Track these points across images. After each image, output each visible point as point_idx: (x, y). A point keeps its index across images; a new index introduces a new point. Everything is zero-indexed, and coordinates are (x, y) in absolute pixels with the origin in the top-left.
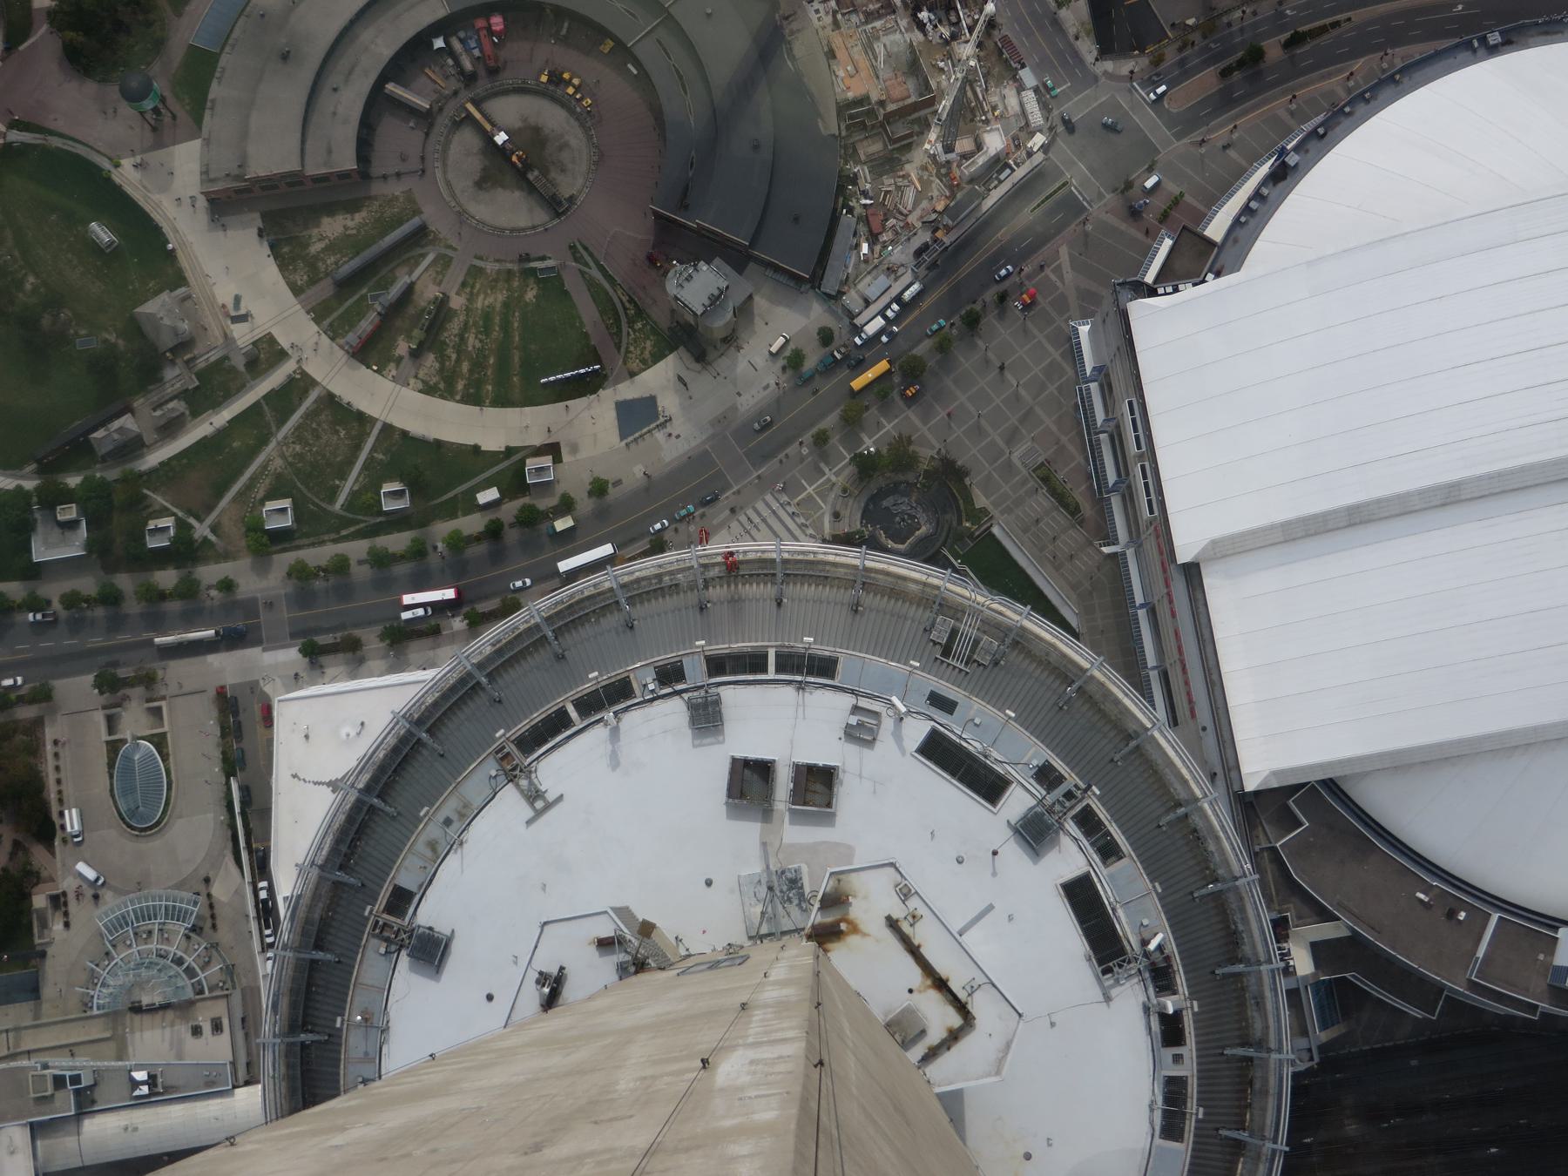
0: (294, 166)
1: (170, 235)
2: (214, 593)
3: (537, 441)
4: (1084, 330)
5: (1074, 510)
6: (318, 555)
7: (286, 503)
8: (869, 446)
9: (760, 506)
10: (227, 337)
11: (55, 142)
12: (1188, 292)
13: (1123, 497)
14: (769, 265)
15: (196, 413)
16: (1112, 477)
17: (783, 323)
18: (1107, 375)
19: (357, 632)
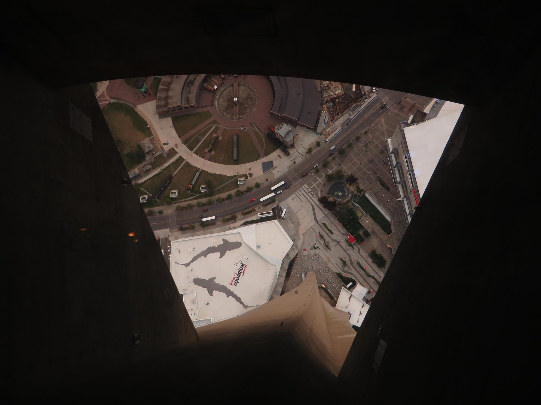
0: (179, 104)
1: (149, 124)
2: (157, 214)
3: (241, 173)
4: (389, 140)
5: (388, 189)
6: (184, 204)
7: (176, 191)
8: (330, 172)
9: (301, 189)
10: (162, 148)
11: (121, 102)
12: (420, 125)
13: (402, 185)
14: (303, 126)
15: (154, 168)
16: (398, 180)
17: (306, 140)
18: (397, 151)
19: (194, 224)
